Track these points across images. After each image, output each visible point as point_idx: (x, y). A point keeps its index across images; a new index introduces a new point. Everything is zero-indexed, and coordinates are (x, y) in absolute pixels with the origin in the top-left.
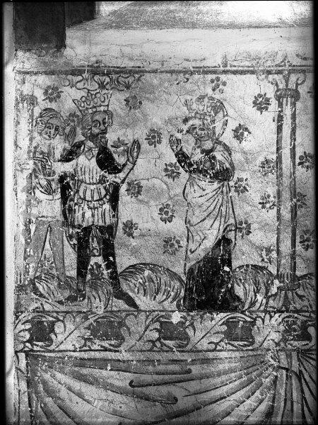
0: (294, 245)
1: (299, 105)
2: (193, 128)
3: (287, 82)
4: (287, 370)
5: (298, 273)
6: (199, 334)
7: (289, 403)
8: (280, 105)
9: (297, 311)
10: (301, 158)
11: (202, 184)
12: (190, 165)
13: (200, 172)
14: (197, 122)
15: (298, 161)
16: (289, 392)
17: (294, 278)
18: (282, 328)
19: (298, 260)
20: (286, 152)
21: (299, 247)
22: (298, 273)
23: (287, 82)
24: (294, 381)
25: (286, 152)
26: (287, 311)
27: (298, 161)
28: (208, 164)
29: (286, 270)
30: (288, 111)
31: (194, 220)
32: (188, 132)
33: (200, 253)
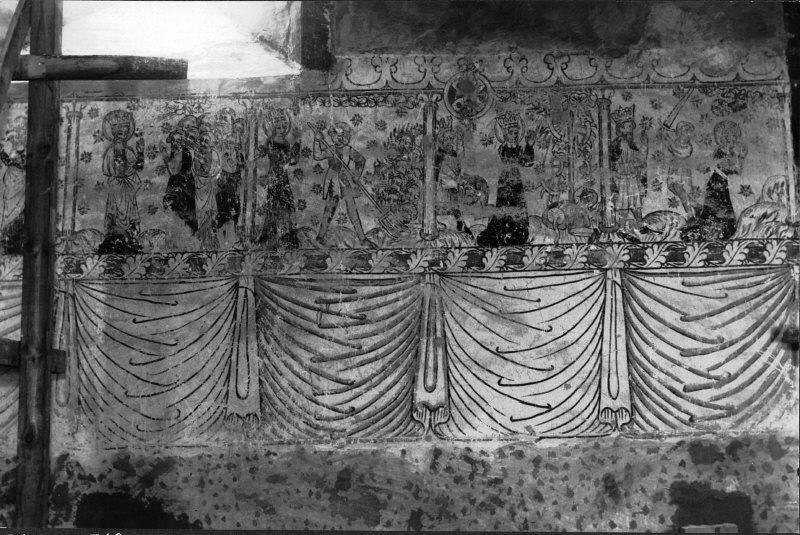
0: (74, 211)
1: (82, 121)
2: (12, 137)
3: (74, 107)
4: (65, 292)
5: (76, 230)
6: (8, 270)
7: (66, 316)
8: (70, 121)
9: (74, 254)
10: (82, 155)
11: (15, 173)
12: (9, 160)
13: (14, 165)
14: (14, 134)
15: (80, 157)
16: (66, 307)
17: (73, 233)
18: (63, 265)
19: (77, 221)
20: (72, 151)
21: (78, 213)
22: (76, 230)
23: (74, 107)
24: (70, 300)
25: (72, 151)
26: (67, 254)
27: (80, 157)
28: (20, 160)
29: (68, 227)
30: (74, 126)
31: (9, 196)
32: (8, 139)
33: (12, 218)
